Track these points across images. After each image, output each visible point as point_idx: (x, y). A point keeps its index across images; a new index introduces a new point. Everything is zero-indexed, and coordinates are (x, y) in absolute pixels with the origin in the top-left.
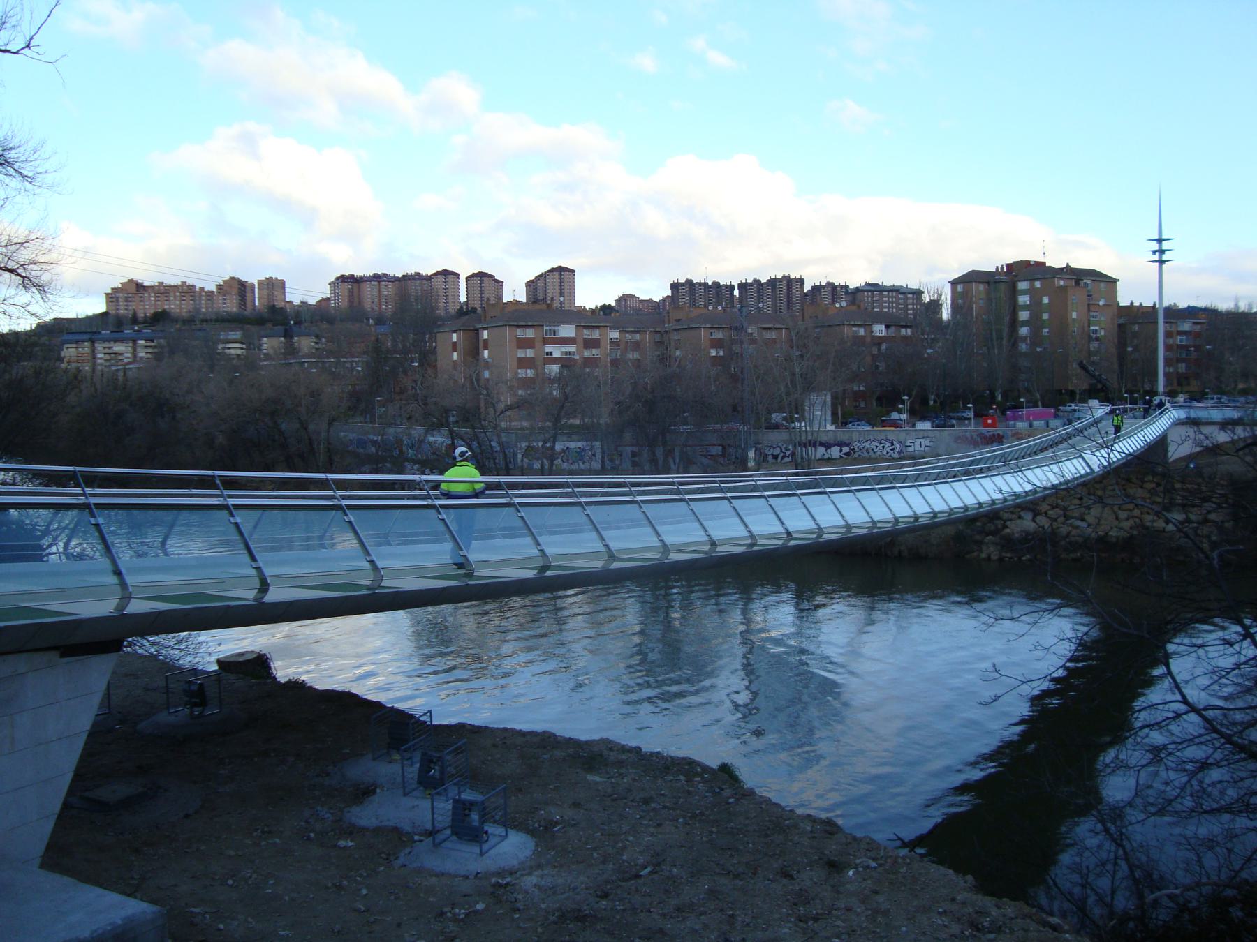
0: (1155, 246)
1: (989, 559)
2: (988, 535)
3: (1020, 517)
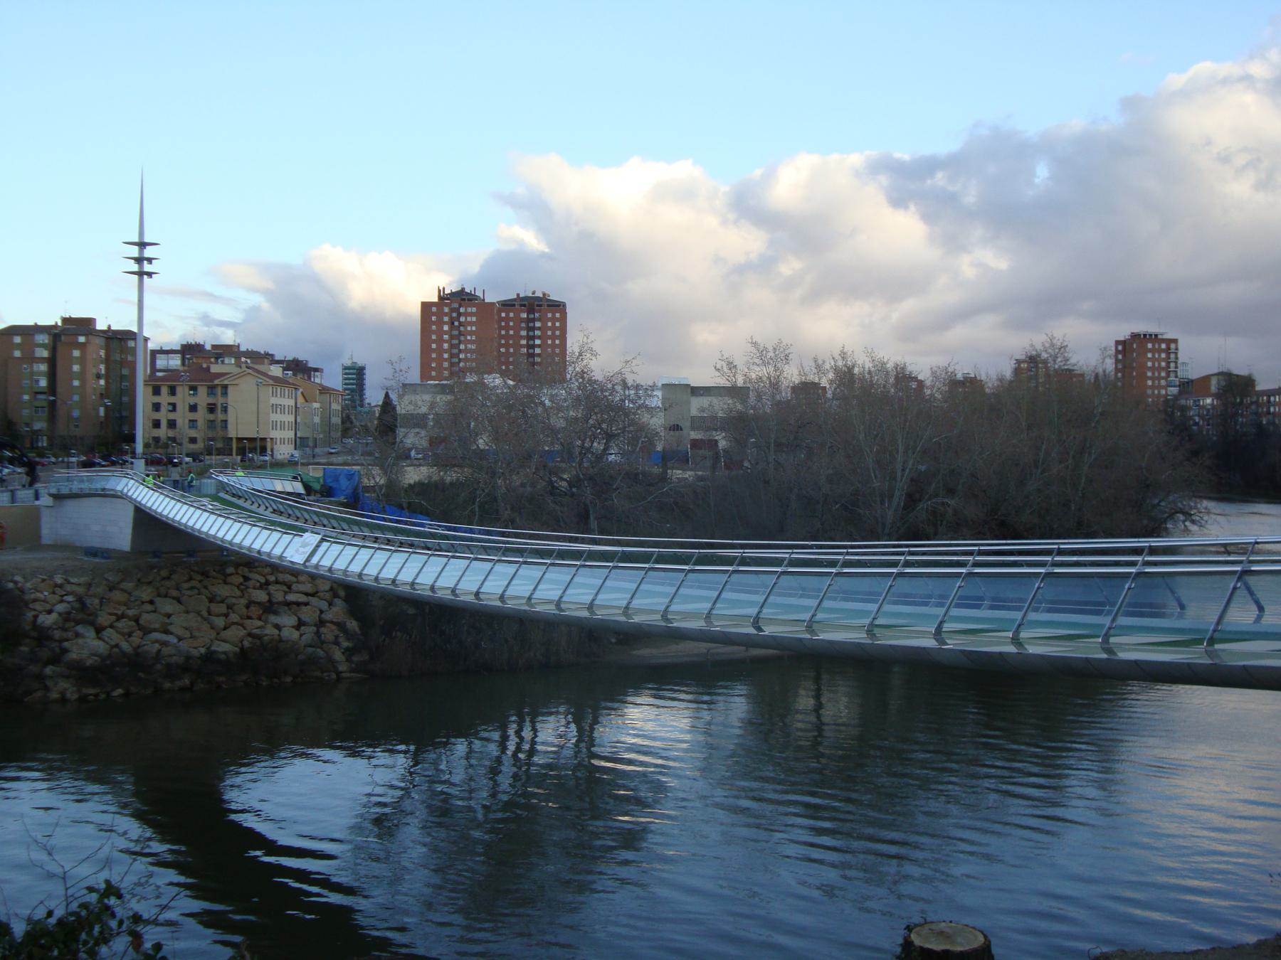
0: (135, 251)
1: (63, 700)
3: (77, 635)
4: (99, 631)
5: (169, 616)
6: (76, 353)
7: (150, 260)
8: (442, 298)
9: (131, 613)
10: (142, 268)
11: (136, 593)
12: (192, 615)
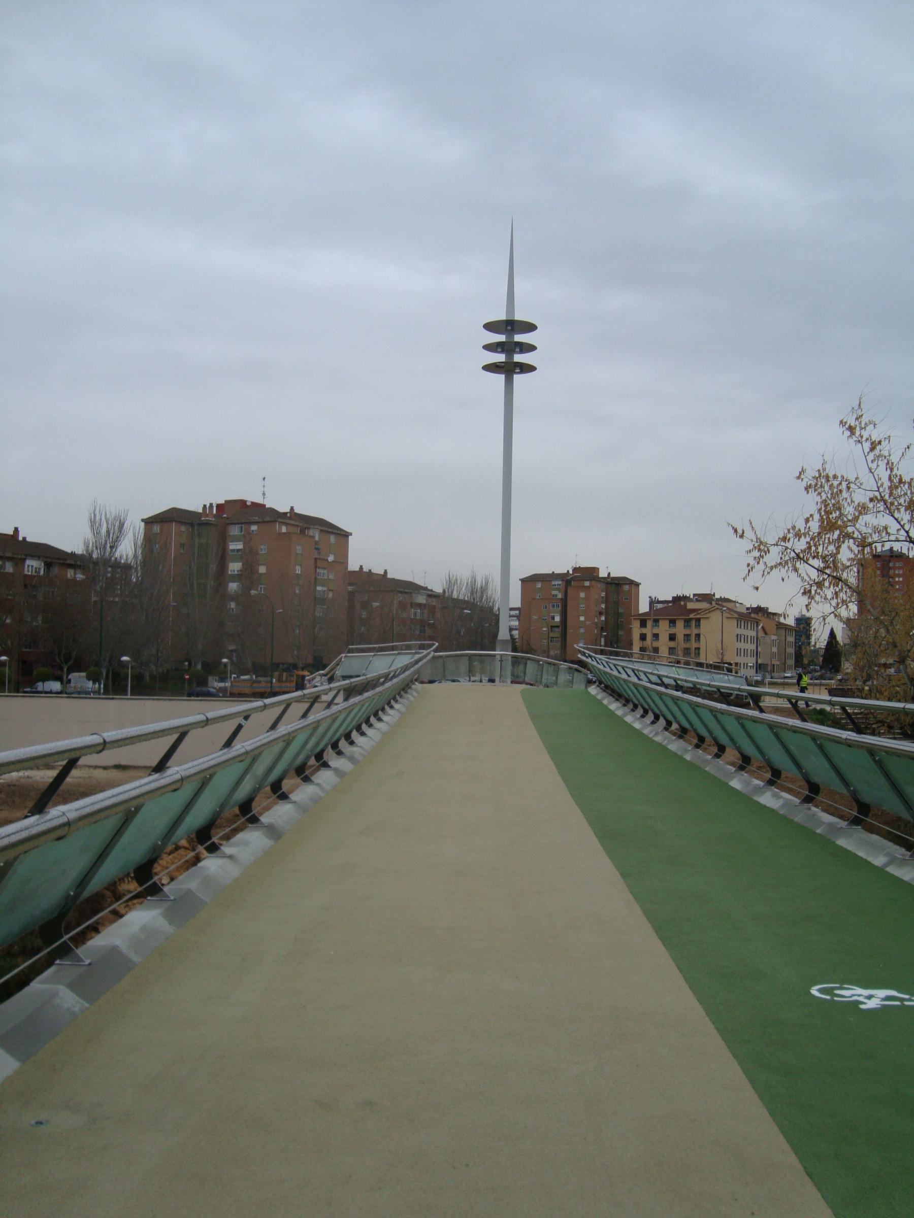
6: (582, 595)
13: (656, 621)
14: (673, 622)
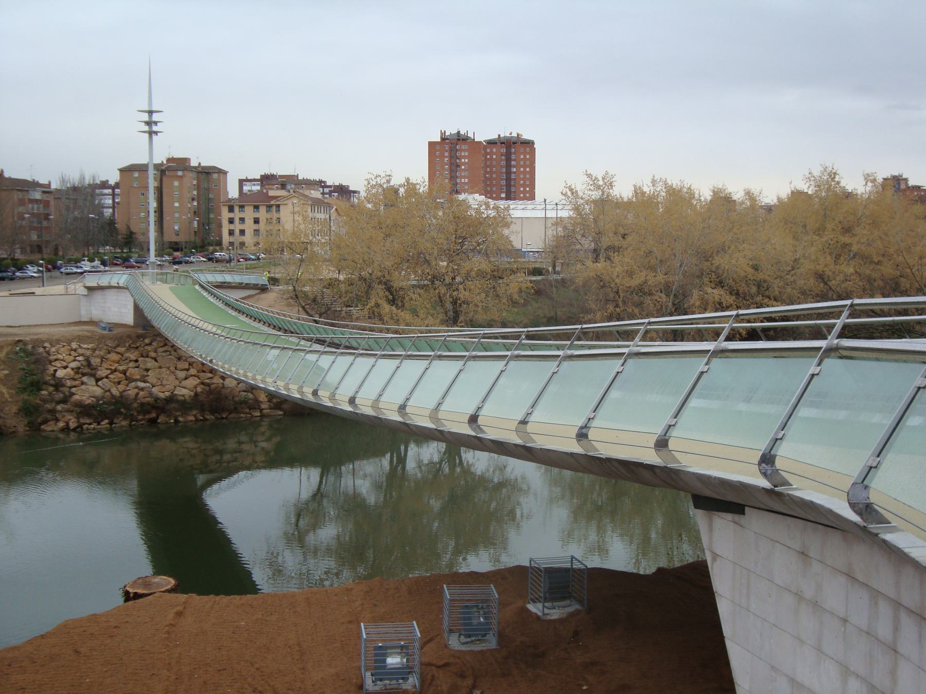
0: (145, 117)
2: (58, 403)
3: (83, 383)
4: (97, 380)
5: (147, 370)
6: (176, 184)
7: (156, 123)
8: (444, 139)
9: (121, 368)
10: (151, 128)
11: (127, 355)
12: (164, 370)
13: (242, 207)
14: (256, 207)
